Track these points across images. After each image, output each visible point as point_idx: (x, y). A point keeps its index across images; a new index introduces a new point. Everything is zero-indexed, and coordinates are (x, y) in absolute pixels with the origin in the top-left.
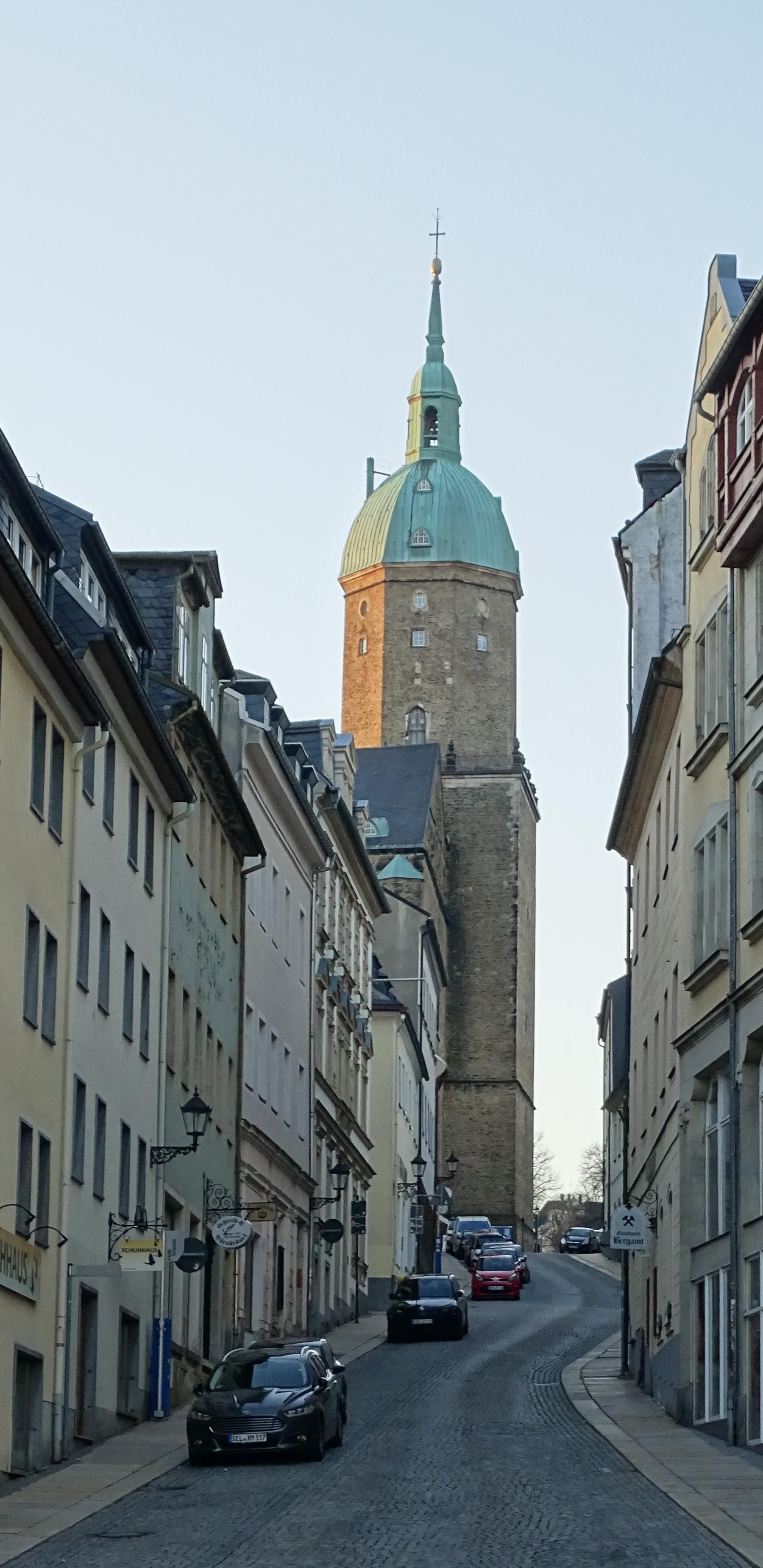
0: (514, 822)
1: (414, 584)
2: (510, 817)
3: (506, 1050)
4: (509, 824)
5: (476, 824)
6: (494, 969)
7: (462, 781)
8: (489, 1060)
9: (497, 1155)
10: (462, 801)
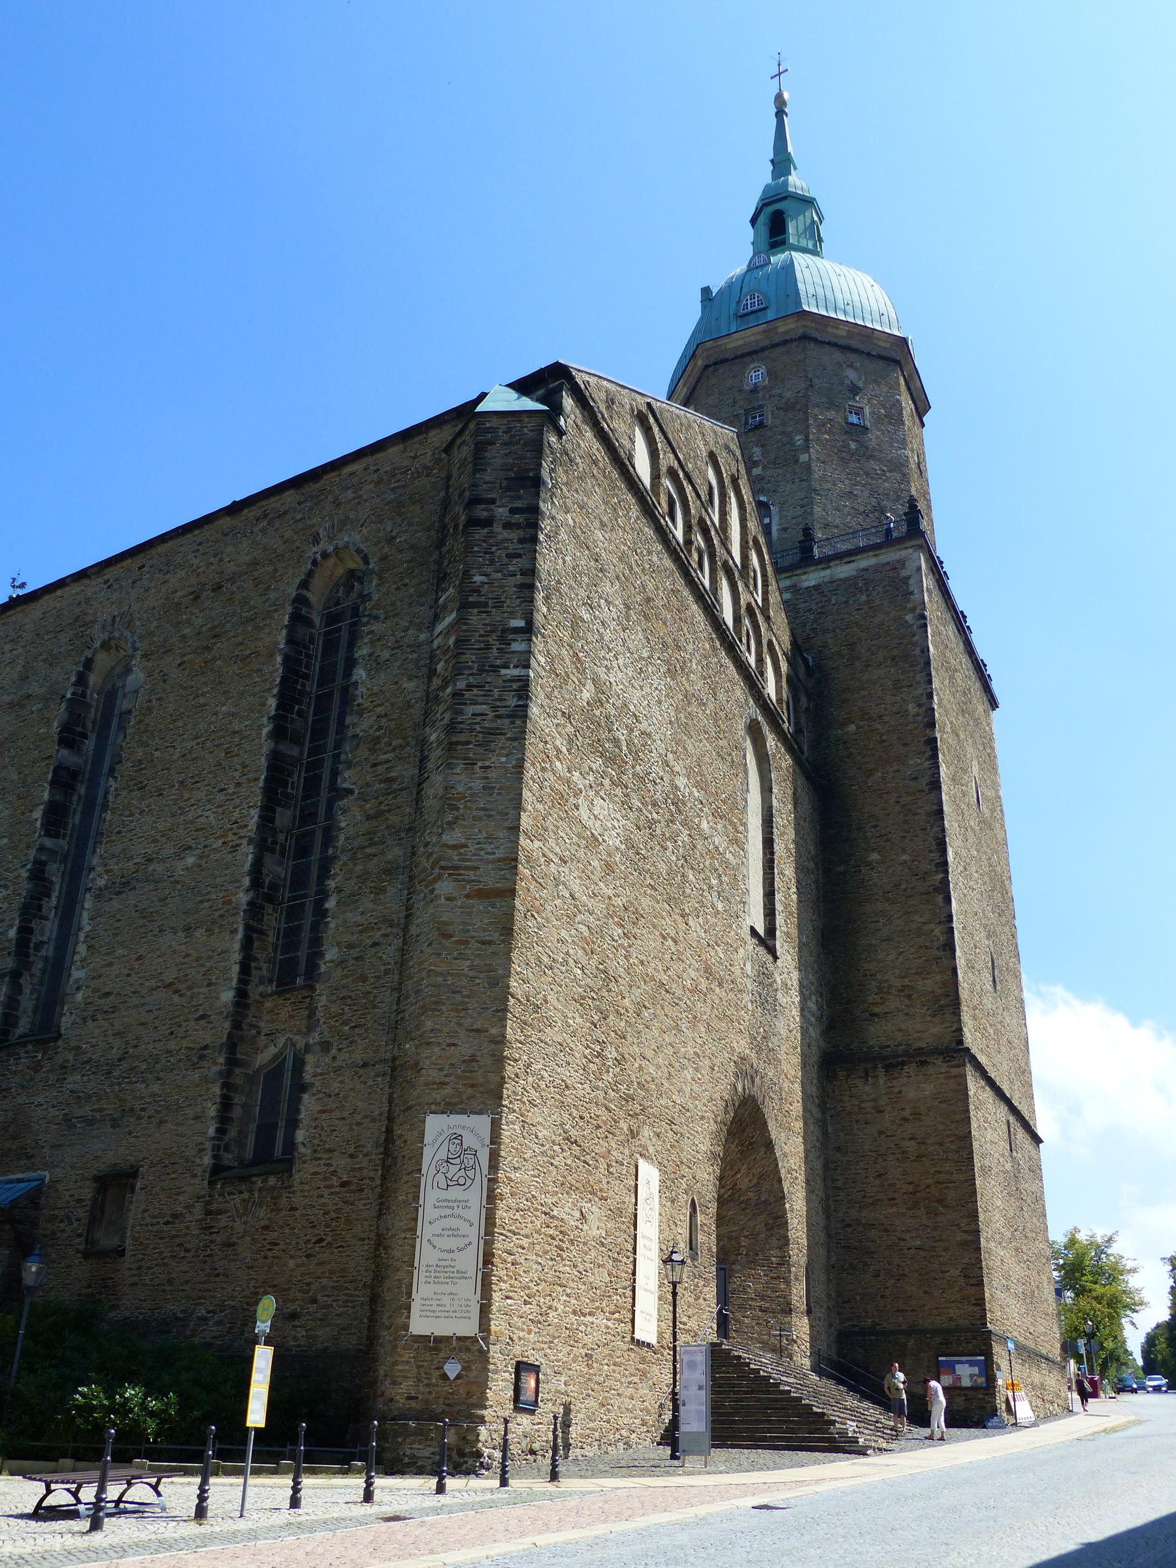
0: (918, 611)
1: (746, 359)
2: (909, 606)
3: (940, 991)
4: (909, 618)
5: (855, 629)
6: (904, 851)
7: (828, 572)
8: (907, 1014)
9: (940, 1201)
10: (830, 600)
